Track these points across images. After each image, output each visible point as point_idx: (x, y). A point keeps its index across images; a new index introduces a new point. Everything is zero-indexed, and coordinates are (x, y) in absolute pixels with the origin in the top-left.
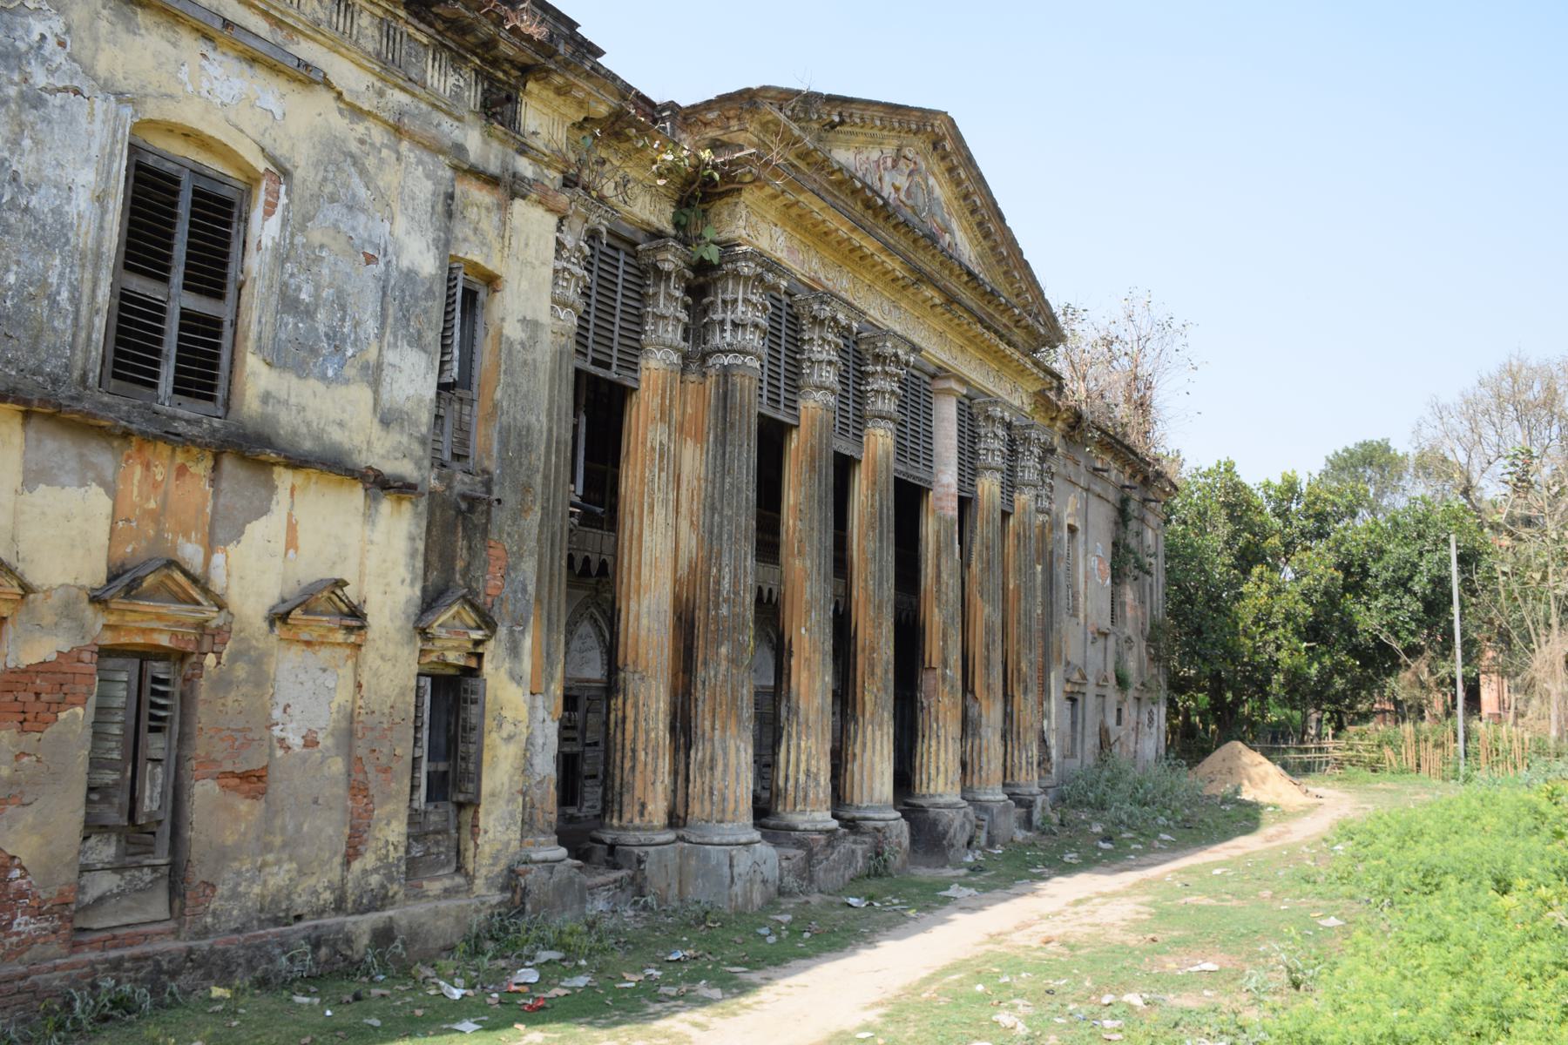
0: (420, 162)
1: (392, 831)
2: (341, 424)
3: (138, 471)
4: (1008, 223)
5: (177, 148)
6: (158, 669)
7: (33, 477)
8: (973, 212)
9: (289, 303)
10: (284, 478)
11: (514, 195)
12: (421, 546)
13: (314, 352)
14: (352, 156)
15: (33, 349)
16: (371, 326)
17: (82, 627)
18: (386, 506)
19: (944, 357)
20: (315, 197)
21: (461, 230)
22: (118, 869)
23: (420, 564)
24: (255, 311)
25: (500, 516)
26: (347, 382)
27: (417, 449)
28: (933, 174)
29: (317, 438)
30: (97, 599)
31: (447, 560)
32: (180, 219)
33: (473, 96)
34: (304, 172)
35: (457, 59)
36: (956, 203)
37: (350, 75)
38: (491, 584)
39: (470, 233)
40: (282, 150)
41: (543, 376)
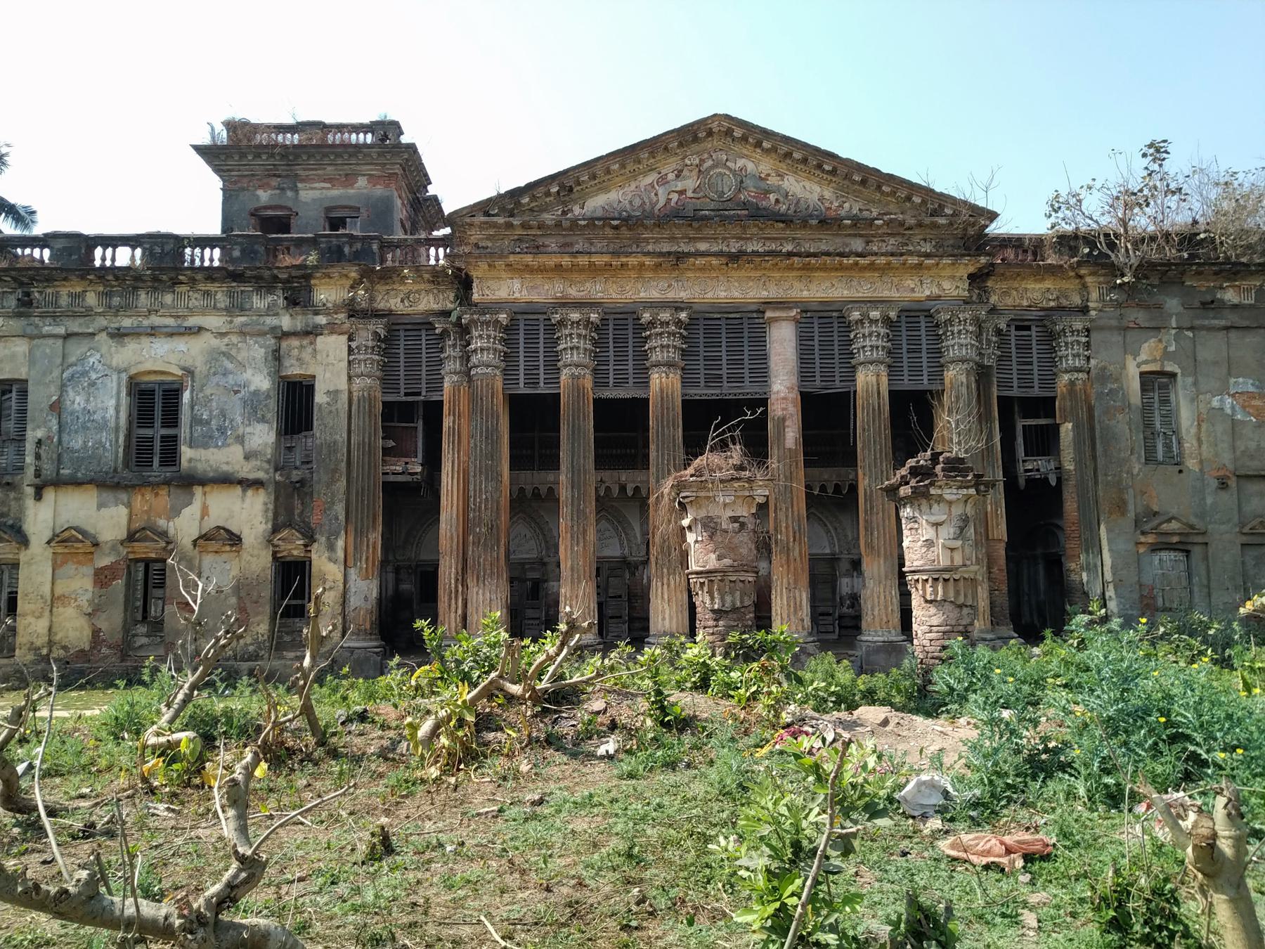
0: (256, 342)
1: (262, 628)
2: (227, 463)
4: (843, 155)
5: (153, 378)
6: (158, 566)
7: (100, 506)
8: (805, 161)
9: (196, 421)
10: (198, 491)
11: (317, 335)
12: (271, 507)
13: (211, 437)
14: (224, 354)
16: (239, 419)
17: (119, 554)
18: (250, 493)
19: (765, 293)
20: (207, 376)
21: (287, 363)
22: (147, 636)
23: (270, 514)
24: (184, 431)
25: (316, 487)
27: (266, 466)
28: (746, 157)
29: (216, 471)
30: (122, 543)
31: (290, 511)
32: (155, 403)
33: (281, 302)
35: (270, 289)
36: (782, 165)
37: (214, 321)
38: (315, 519)
39: (294, 362)
41: (344, 416)
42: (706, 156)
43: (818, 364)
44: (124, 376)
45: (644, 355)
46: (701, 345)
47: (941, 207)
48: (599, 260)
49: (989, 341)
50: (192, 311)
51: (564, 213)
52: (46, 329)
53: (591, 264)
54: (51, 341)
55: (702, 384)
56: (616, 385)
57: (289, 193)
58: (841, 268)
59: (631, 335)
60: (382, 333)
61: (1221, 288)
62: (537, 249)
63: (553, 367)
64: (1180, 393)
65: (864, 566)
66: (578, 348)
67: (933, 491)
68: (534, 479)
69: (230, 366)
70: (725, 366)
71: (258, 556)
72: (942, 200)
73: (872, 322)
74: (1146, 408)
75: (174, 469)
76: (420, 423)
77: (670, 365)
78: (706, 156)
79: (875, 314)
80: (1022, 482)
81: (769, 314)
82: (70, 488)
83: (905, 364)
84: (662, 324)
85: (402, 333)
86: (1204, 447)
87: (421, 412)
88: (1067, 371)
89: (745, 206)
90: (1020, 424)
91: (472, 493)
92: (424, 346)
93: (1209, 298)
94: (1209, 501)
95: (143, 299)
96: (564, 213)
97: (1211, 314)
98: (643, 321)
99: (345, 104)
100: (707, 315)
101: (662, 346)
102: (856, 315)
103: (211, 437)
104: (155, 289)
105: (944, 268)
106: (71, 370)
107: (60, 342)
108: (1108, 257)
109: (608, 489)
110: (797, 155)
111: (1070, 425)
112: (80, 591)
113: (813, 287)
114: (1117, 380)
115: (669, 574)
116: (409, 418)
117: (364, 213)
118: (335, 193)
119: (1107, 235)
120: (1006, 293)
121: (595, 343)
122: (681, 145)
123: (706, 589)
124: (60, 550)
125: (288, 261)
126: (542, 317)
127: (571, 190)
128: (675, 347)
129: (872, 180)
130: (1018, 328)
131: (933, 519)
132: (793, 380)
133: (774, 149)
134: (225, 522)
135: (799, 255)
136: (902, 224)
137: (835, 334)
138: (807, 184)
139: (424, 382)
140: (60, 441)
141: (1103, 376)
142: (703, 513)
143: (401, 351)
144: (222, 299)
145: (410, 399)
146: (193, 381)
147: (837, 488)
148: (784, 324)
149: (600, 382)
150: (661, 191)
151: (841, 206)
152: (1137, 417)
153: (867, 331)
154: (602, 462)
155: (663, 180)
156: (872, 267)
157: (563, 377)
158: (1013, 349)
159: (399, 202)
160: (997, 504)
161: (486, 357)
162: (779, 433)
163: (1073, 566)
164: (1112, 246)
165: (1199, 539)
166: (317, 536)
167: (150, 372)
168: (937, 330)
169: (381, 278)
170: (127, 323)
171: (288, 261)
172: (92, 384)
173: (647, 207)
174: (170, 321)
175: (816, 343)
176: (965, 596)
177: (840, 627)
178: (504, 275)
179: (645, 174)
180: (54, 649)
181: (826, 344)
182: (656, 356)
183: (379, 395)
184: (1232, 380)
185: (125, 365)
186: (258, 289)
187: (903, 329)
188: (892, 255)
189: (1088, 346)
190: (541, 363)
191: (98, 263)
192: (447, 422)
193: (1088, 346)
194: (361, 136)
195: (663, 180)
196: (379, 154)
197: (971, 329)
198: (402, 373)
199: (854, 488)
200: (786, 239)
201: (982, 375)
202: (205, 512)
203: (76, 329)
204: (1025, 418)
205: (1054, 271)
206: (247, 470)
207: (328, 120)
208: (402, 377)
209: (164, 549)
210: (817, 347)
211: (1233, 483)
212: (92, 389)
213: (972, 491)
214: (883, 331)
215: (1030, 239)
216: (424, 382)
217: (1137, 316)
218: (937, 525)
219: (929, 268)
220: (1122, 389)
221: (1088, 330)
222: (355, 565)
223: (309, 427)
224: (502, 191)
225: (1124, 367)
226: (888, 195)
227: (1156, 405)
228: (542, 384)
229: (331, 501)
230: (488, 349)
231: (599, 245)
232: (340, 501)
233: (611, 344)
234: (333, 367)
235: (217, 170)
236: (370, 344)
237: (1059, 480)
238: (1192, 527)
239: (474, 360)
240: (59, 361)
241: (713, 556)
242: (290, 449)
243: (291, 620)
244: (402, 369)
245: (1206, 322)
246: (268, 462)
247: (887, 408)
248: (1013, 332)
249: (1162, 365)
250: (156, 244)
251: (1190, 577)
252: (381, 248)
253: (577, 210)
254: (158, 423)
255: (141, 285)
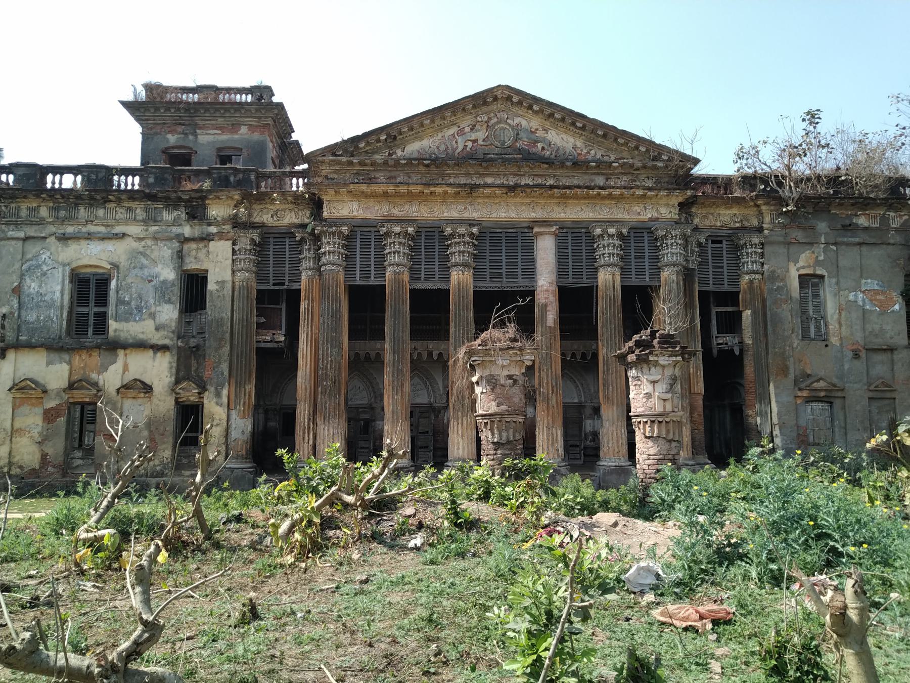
1: (166, 453)
2: (143, 333)
3: (78, 357)
4: (591, 116)
5: (89, 270)
6: (90, 408)
7: (49, 363)
8: (563, 120)
9: (120, 302)
10: (121, 353)
11: (209, 241)
12: (175, 365)
13: (131, 314)
14: (141, 253)
15: (48, 333)
16: (152, 301)
18: (159, 355)
19: (533, 215)
21: (187, 260)
23: (174, 370)
24: (111, 309)
25: (208, 352)
26: (144, 320)
27: (171, 335)
28: (521, 116)
29: (134, 338)
30: (64, 390)
31: (188, 368)
32: (90, 289)
33: (183, 216)
34: (123, 262)
35: (176, 207)
37: (134, 230)
38: (207, 374)
40: (115, 260)
41: (229, 299)
42: (492, 115)
43: (570, 266)
44: (68, 269)
45: (447, 258)
46: (488, 251)
47: (660, 154)
48: (415, 189)
49: (692, 253)
50: (118, 222)
51: (390, 155)
52: (11, 234)
53: (409, 192)
54: (13, 243)
55: (488, 279)
56: (426, 279)
57: (191, 137)
58: (588, 197)
59: (437, 244)
60: (257, 240)
61: (856, 215)
62: (371, 181)
63: (381, 265)
64: (827, 289)
65: (603, 412)
66: (399, 252)
67: (651, 358)
68: (367, 346)
69: (145, 262)
70: (504, 267)
71: (164, 401)
72: (661, 148)
73: (610, 236)
74: (803, 300)
75: (103, 337)
76: (284, 307)
77: (465, 265)
78: (492, 115)
79: (612, 231)
80: (715, 352)
81: (536, 230)
82: (27, 350)
83: (633, 267)
84: (459, 235)
85: (271, 240)
86: (843, 328)
87: (285, 297)
88: (747, 273)
89: (520, 151)
90: (714, 310)
91: (321, 357)
92: (287, 250)
93: (847, 222)
94: (846, 367)
95: (82, 212)
96: (390, 155)
97: (849, 234)
98: (446, 233)
99: (232, 73)
100: (492, 230)
101: (460, 252)
102: (598, 231)
103: (131, 314)
104: (91, 205)
105: (661, 198)
106: (28, 264)
107: (20, 243)
108: (777, 192)
109: (419, 354)
110: (557, 116)
111: (749, 312)
112: (33, 426)
113: (568, 210)
114: (782, 280)
115: (462, 416)
116: (276, 302)
117: (245, 153)
118: (224, 138)
119: (776, 177)
120: (705, 217)
121: (412, 249)
122: (474, 107)
123: (488, 427)
124: (18, 395)
125: (189, 186)
126: (373, 230)
127: (395, 138)
128: (468, 252)
129: (611, 134)
130: (713, 242)
131: (652, 378)
132: (553, 277)
133: (541, 111)
134: (140, 376)
135: (558, 187)
136: (632, 166)
137: (584, 244)
138: (564, 136)
139: (287, 275)
140: (19, 316)
141: (773, 277)
142: (487, 372)
143: (271, 253)
144: (140, 213)
145: (277, 287)
146: (118, 273)
147: (584, 356)
148: (547, 237)
149: (414, 278)
150: (460, 140)
151: (588, 153)
152: (796, 307)
153: (606, 243)
154: (416, 334)
155: (461, 132)
156: (610, 197)
157: (388, 273)
158: (710, 257)
159: (271, 145)
160: (697, 368)
161: (331, 258)
162: (542, 314)
163: (750, 412)
164: (780, 184)
165: (839, 394)
166: (208, 387)
167: (86, 266)
168: (656, 243)
169: (257, 200)
170: (70, 230)
171: (189, 186)
172: (44, 274)
173: (450, 151)
174: (102, 229)
175: (570, 251)
176: (674, 434)
177: (585, 455)
178: (346, 199)
179: (448, 127)
180: (13, 468)
181: (577, 252)
182: (455, 259)
183: (254, 285)
184: (863, 281)
185: (68, 261)
186: (167, 207)
187: (632, 241)
188: (625, 188)
189: (762, 255)
190: (372, 263)
191: (49, 186)
192: (303, 305)
193: (762, 255)
194: (244, 96)
195: (461, 132)
196: (257, 110)
197: (680, 242)
198: (271, 269)
199: (595, 356)
200: (549, 176)
201: (687, 275)
202: (126, 368)
203: (33, 234)
204: (718, 307)
205: (739, 201)
206: (158, 338)
207: (220, 84)
208: (271, 271)
209: (96, 395)
210: (570, 254)
211: (863, 354)
212: (44, 278)
213: (679, 358)
214: (617, 243)
215: (723, 178)
216: (287, 275)
217: (798, 235)
218: (654, 382)
219: (651, 198)
220: (786, 286)
221: (762, 244)
222: (235, 408)
223: (203, 307)
224: (346, 138)
225: (788, 271)
226: (622, 145)
227: (810, 298)
228: (372, 278)
229: (219, 362)
230: (334, 252)
231: (415, 178)
232: (225, 361)
233: (423, 250)
234: (220, 264)
235: (138, 119)
236: (248, 247)
237: (741, 351)
238: (834, 385)
239: (324, 260)
240: (19, 257)
241: (494, 404)
242: (189, 323)
243: (188, 448)
244: (271, 265)
245: (845, 240)
246: (173, 332)
247: (620, 298)
248: (710, 245)
249: (815, 270)
250: (92, 172)
251: (832, 421)
252: (257, 178)
253: (399, 153)
254: (92, 303)
255: (81, 202)
